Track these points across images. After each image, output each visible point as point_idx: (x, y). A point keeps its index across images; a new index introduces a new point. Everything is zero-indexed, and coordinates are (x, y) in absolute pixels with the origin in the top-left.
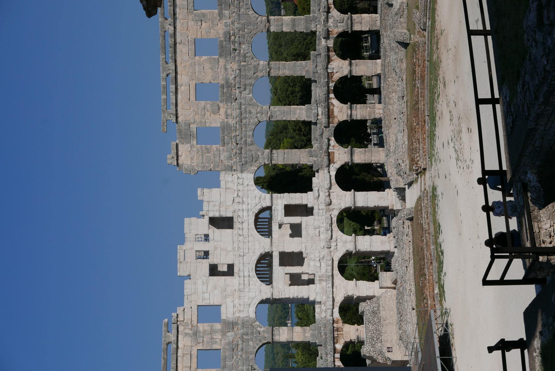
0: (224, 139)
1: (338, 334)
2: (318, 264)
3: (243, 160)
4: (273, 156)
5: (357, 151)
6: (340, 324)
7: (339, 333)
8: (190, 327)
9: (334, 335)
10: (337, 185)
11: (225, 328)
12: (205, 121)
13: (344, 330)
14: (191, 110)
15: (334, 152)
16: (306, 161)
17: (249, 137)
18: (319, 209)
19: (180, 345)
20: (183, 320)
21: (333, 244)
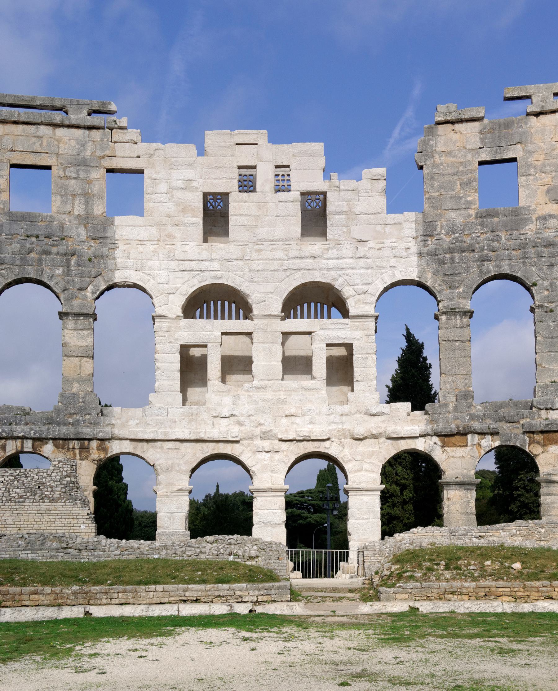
0: (493, 216)
1: (74, 448)
2: (226, 413)
3: (448, 256)
4: (456, 319)
5: (469, 495)
6: (96, 455)
7: (77, 452)
8: (99, 153)
9: (73, 439)
10: (393, 453)
11: (94, 222)
12: (530, 175)
13: (84, 462)
14: (554, 143)
15: (466, 446)
16: (446, 388)
17: (497, 266)
18: (342, 415)
19: (60, 132)
20: (113, 140)
21: (266, 444)
